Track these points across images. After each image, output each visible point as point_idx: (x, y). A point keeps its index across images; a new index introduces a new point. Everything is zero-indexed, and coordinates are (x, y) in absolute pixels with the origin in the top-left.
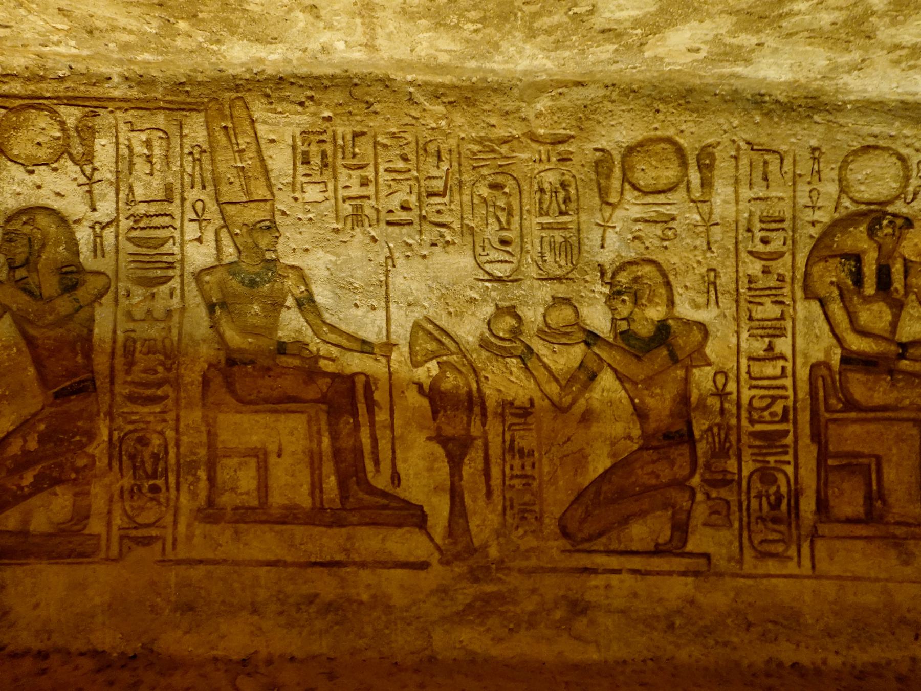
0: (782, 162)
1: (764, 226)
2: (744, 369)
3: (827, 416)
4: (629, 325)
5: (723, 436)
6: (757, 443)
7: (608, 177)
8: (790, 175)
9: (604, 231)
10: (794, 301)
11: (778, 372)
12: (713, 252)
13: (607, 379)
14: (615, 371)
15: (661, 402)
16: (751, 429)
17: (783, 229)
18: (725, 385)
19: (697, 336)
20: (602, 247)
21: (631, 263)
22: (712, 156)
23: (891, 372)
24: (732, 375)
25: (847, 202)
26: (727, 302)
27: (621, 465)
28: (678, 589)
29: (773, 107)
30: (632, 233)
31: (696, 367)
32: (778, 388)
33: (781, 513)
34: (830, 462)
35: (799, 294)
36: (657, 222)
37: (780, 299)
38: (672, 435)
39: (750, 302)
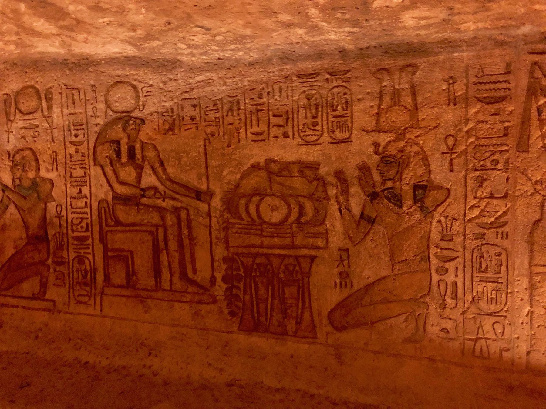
0: (79, 94)
1: (75, 128)
2: (69, 204)
3: (107, 229)
4: (20, 181)
5: (61, 238)
6: (76, 243)
7: (10, 107)
8: (83, 100)
9: (9, 134)
10: (89, 166)
11: (83, 205)
12: (54, 143)
13: (12, 209)
14: (16, 205)
15: (34, 221)
16: (72, 235)
17: (83, 129)
18: (61, 213)
19: (48, 186)
20: (9, 142)
21: (21, 150)
22: (51, 93)
23: (137, 205)
24: (64, 207)
25: (111, 113)
26: (61, 169)
27: (19, 252)
28: (41, 318)
29: (72, 65)
30: (20, 135)
31: (49, 202)
32: (84, 213)
33: (87, 281)
34: (110, 254)
35: (92, 163)
36: (30, 128)
37: (84, 166)
38: (38, 238)
39: (71, 168)
